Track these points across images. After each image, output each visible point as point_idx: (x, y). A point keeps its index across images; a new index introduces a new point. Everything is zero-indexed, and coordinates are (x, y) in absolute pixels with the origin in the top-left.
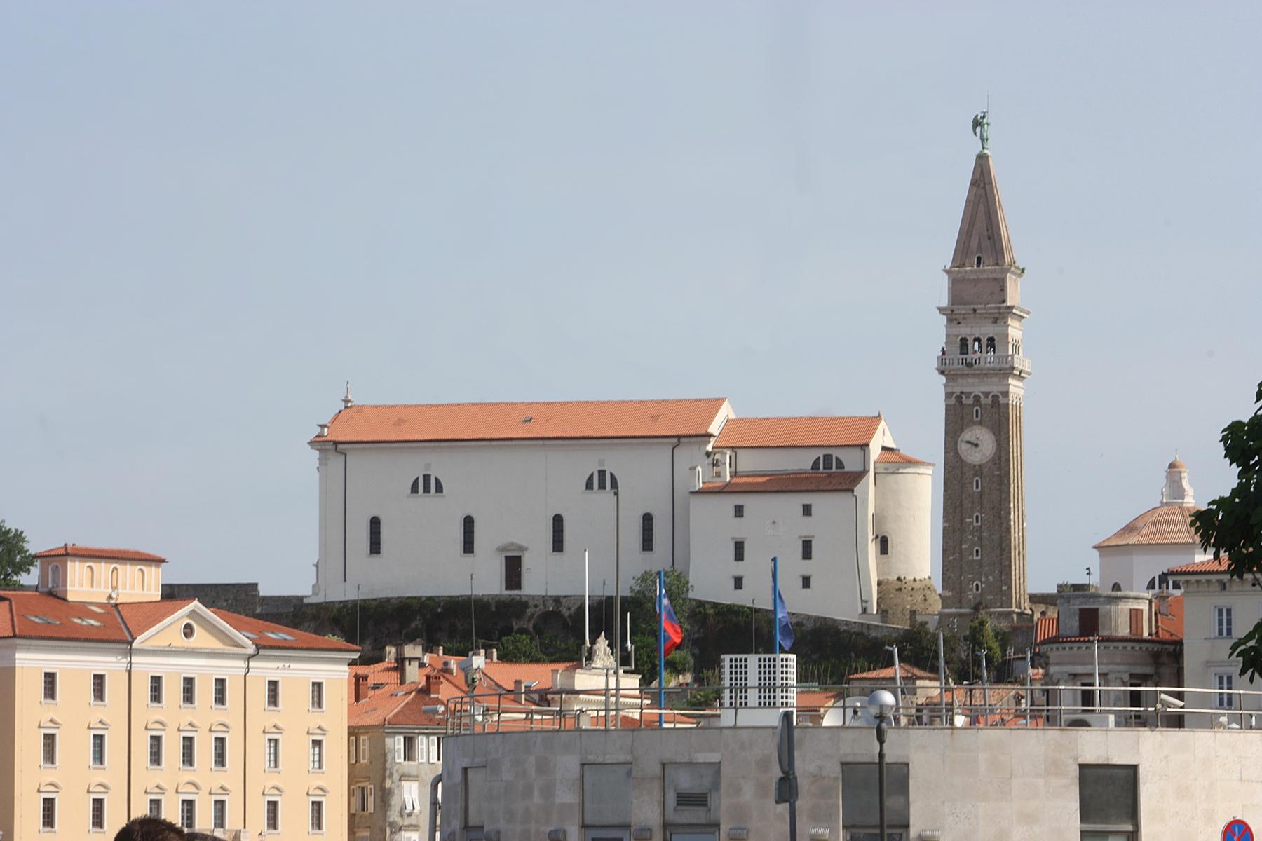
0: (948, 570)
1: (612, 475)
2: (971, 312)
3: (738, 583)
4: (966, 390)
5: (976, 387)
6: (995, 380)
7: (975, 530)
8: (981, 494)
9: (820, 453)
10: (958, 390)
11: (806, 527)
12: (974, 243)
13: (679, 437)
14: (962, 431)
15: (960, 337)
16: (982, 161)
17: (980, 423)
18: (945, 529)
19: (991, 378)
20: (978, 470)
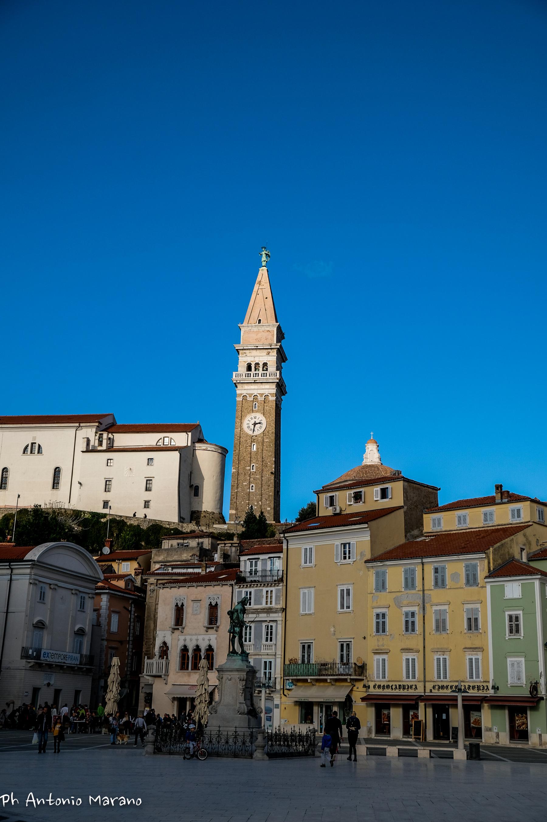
0: (234, 498)
1: (39, 446)
3: (106, 504)
6: (267, 386)
7: (252, 474)
8: (257, 452)
10: (244, 392)
11: (150, 472)
15: (247, 363)
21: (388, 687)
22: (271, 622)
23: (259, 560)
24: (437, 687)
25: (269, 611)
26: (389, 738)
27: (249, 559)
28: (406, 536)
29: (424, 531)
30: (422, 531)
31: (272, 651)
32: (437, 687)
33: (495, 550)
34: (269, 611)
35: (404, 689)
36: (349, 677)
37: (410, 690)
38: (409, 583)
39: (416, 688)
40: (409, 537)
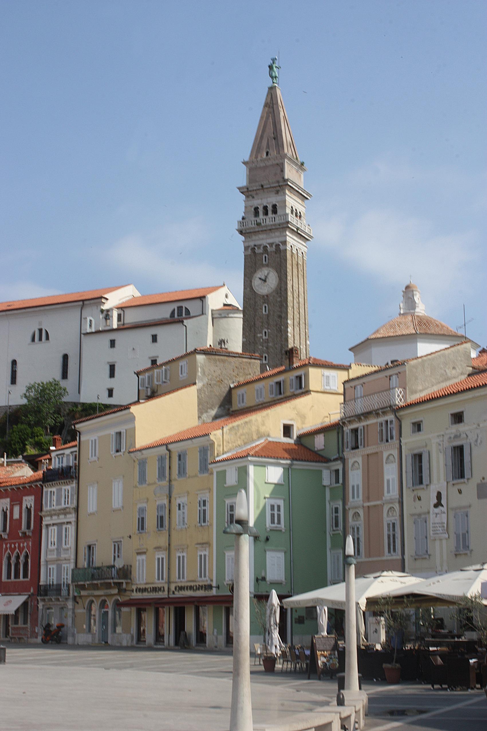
2: (260, 187)
3: (110, 393)
4: (258, 243)
5: (264, 240)
6: (277, 234)
8: (268, 316)
9: (175, 306)
10: (252, 244)
12: (264, 143)
13: (83, 301)
14: (255, 271)
16: (272, 90)
17: (267, 266)
18: (243, 343)
19: (274, 233)
20: (266, 298)
21: (145, 590)
22: (69, 524)
23: (65, 456)
24: (177, 589)
25: (65, 512)
26: (145, 646)
27: (57, 455)
28: (199, 417)
29: (231, 410)
30: (229, 410)
31: (66, 556)
32: (177, 589)
33: (231, 429)
34: (65, 512)
35: (142, 592)
36: (112, 581)
37: (160, 593)
38: (161, 475)
39: (164, 590)
40: (205, 419)
